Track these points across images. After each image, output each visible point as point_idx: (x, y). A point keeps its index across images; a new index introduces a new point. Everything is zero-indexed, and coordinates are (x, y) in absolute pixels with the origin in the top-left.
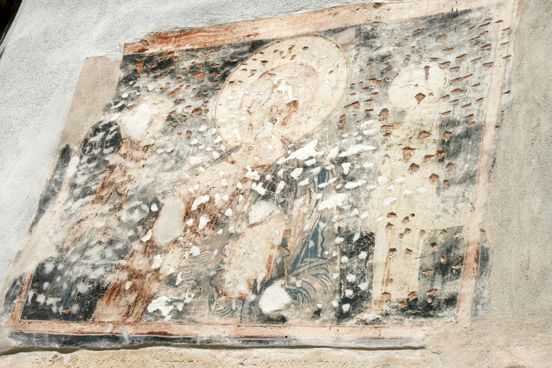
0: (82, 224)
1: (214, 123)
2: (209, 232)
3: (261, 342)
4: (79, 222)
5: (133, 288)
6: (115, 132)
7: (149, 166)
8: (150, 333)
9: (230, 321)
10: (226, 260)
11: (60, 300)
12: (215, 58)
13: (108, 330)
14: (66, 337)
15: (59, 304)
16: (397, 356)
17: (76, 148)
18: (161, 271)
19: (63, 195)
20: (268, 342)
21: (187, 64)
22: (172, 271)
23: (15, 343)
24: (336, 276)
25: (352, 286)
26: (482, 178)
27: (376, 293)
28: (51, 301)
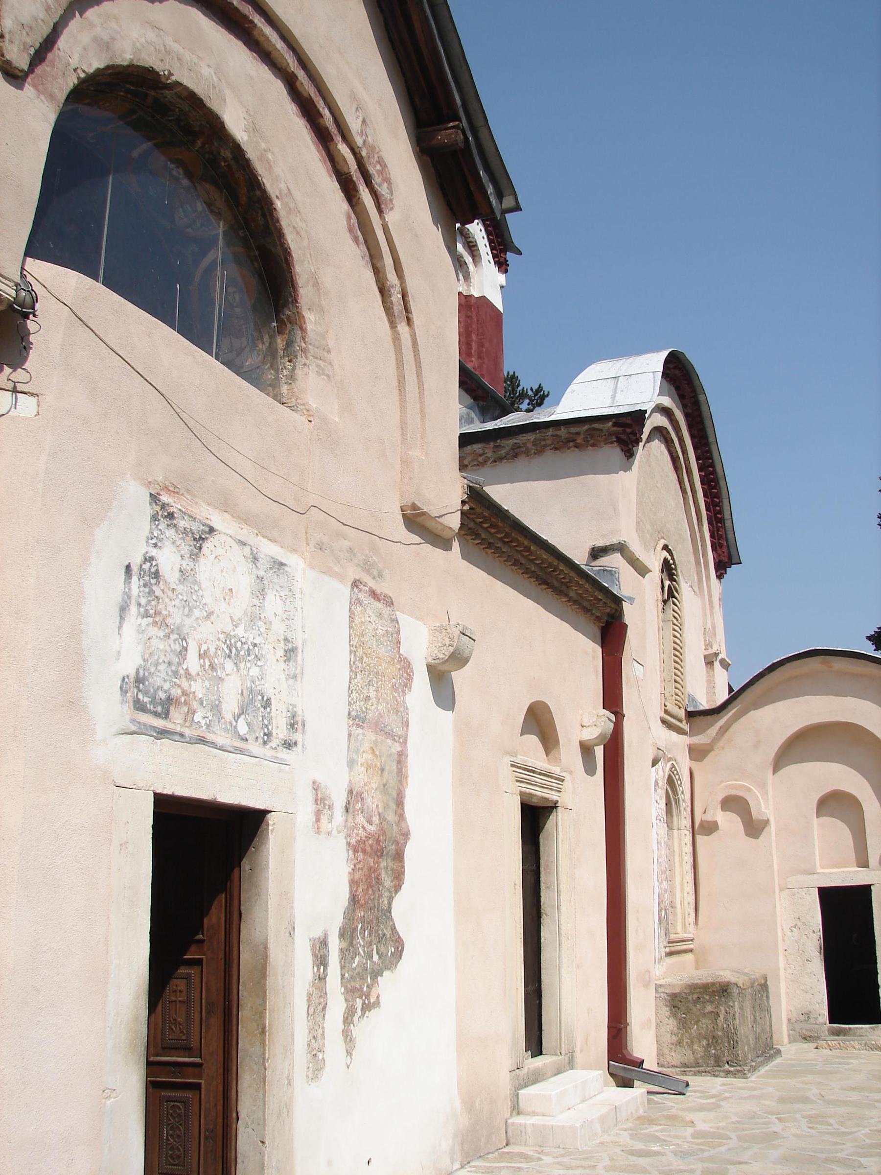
0: (151, 640)
1: (199, 584)
2: (210, 672)
3: (241, 751)
4: (149, 639)
5: (186, 703)
6: (156, 567)
7: (177, 608)
8: (198, 736)
9: (228, 736)
10: (221, 695)
11: (150, 700)
12: (195, 527)
13: (178, 729)
14: (159, 729)
15: (151, 702)
16: (283, 768)
17: (135, 569)
18: (196, 694)
19: (133, 609)
20: (243, 751)
21: (182, 524)
22: (200, 696)
23: (133, 728)
24: (261, 719)
25: (267, 726)
26: (299, 679)
27: (274, 732)
28: (146, 699)
